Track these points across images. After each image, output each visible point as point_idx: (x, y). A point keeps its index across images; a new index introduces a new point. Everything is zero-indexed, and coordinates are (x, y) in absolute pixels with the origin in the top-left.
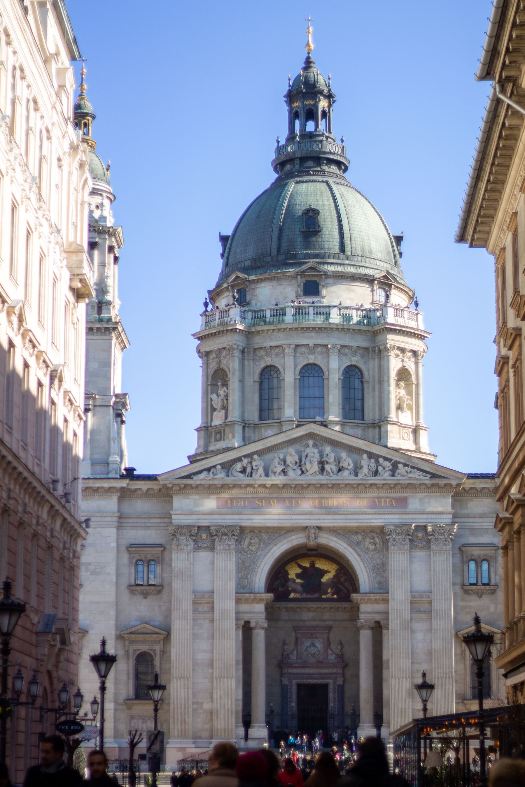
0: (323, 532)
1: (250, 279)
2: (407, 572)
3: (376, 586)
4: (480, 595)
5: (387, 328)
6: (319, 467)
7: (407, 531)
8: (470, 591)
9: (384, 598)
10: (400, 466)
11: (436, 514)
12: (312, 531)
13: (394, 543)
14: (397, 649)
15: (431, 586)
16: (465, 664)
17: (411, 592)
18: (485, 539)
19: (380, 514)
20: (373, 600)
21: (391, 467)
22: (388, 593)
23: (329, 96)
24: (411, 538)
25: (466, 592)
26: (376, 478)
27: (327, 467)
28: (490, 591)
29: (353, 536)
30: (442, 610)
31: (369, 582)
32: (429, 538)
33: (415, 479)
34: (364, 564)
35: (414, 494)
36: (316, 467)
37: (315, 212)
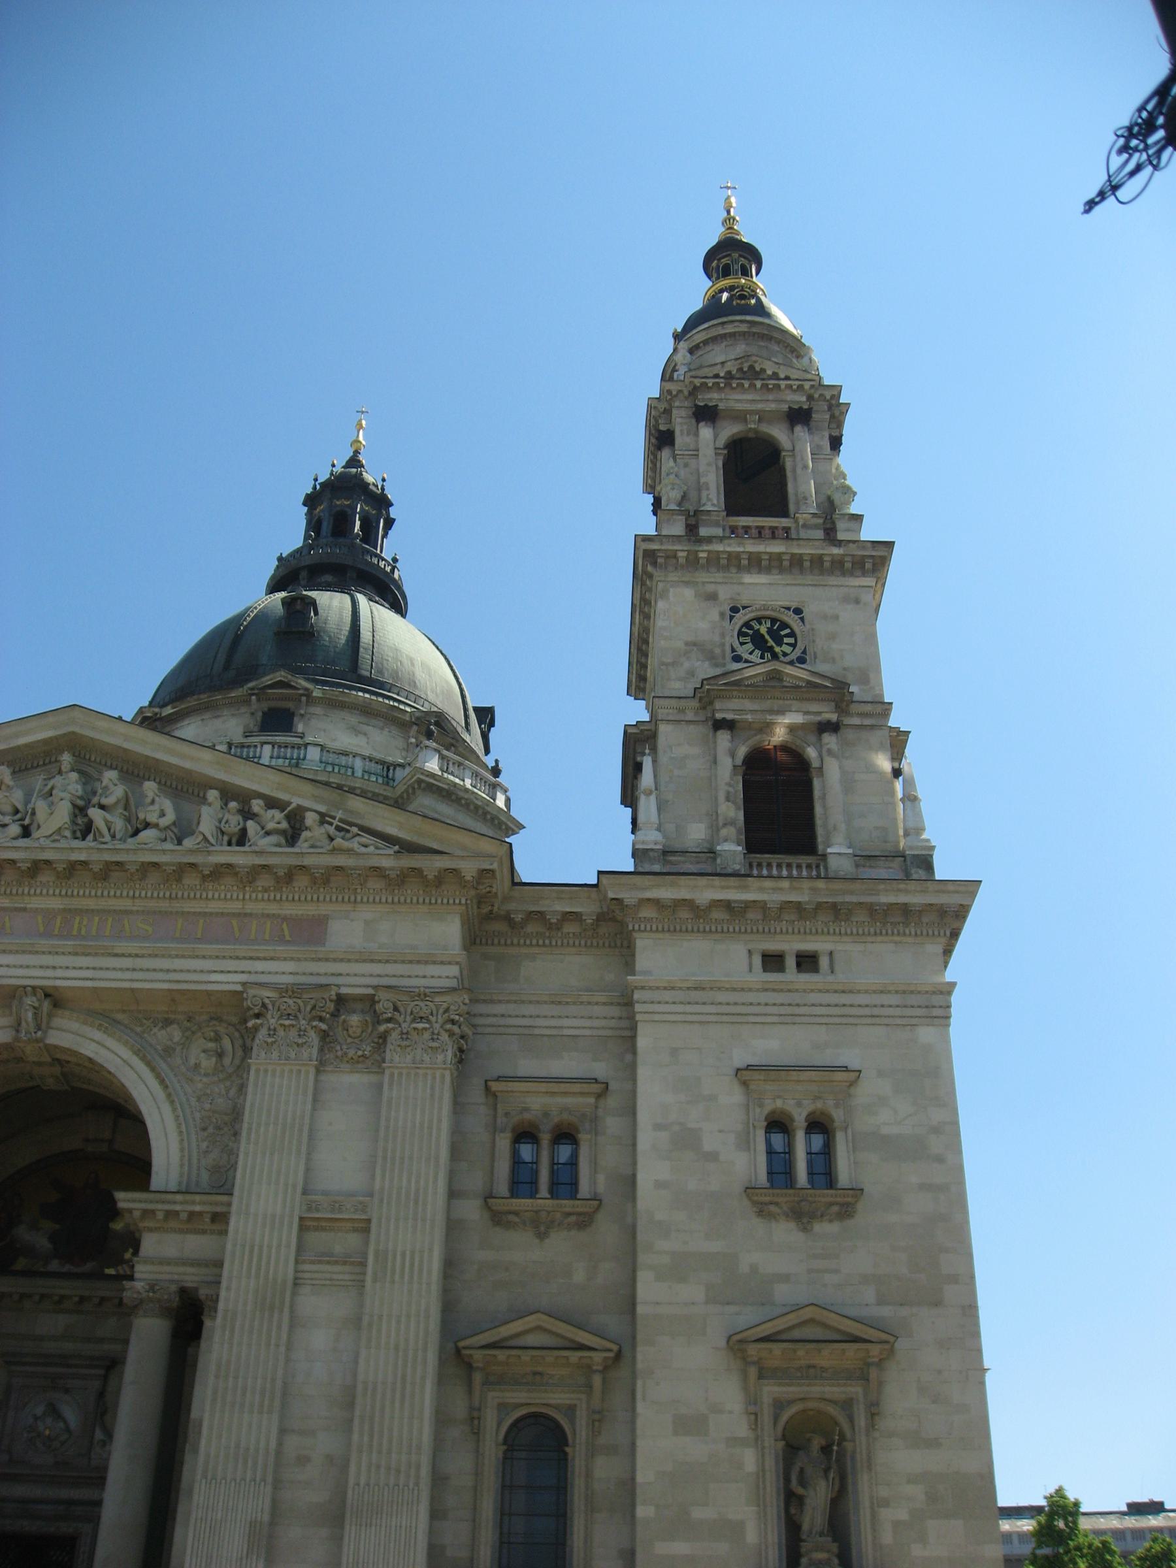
0: (67, 1013)
1: (163, 714)
2: (301, 1130)
3: (205, 1176)
4: (541, 1228)
5: (420, 781)
6: (74, 823)
7: (314, 1007)
8: (511, 1218)
9: (219, 1209)
10: (310, 819)
11: (411, 962)
12: (29, 1000)
13: (270, 1040)
14: (236, 1378)
15: (373, 1177)
16: (477, 1452)
17: (305, 1192)
18: (567, 1065)
19: (237, 958)
20: (184, 1216)
21: (284, 825)
22: (231, 1194)
23: (381, 502)
24: (324, 1026)
25: (498, 1219)
26: (238, 848)
27: (95, 813)
28: (573, 1218)
29: (155, 1030)
30: (403, 1254)
31: (182, 1166)
32: (382, 1028)
33: (349, 851)
34: (174, 1110)
35: (349, 907)
36: (63, 814)
37: (307, 601)
